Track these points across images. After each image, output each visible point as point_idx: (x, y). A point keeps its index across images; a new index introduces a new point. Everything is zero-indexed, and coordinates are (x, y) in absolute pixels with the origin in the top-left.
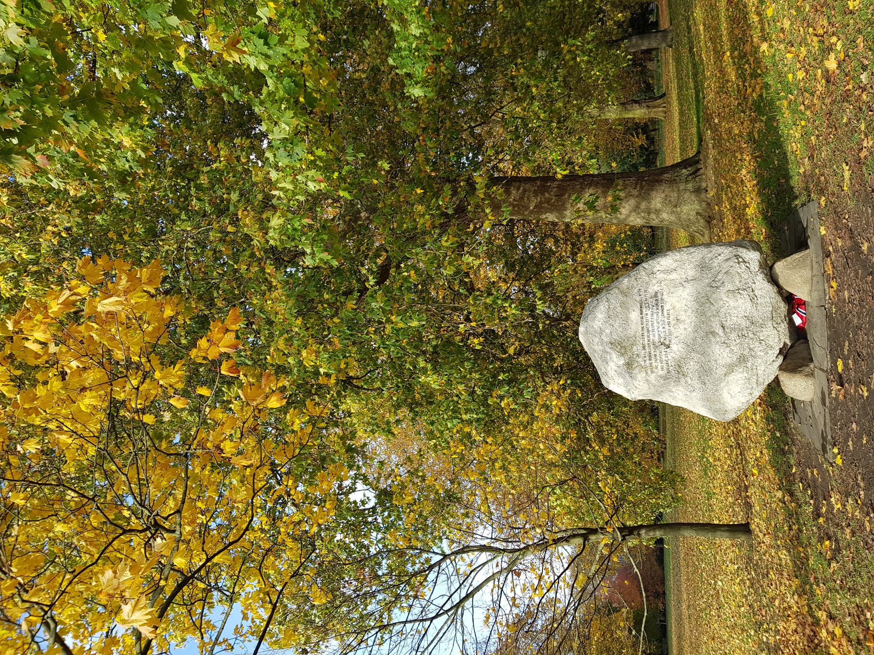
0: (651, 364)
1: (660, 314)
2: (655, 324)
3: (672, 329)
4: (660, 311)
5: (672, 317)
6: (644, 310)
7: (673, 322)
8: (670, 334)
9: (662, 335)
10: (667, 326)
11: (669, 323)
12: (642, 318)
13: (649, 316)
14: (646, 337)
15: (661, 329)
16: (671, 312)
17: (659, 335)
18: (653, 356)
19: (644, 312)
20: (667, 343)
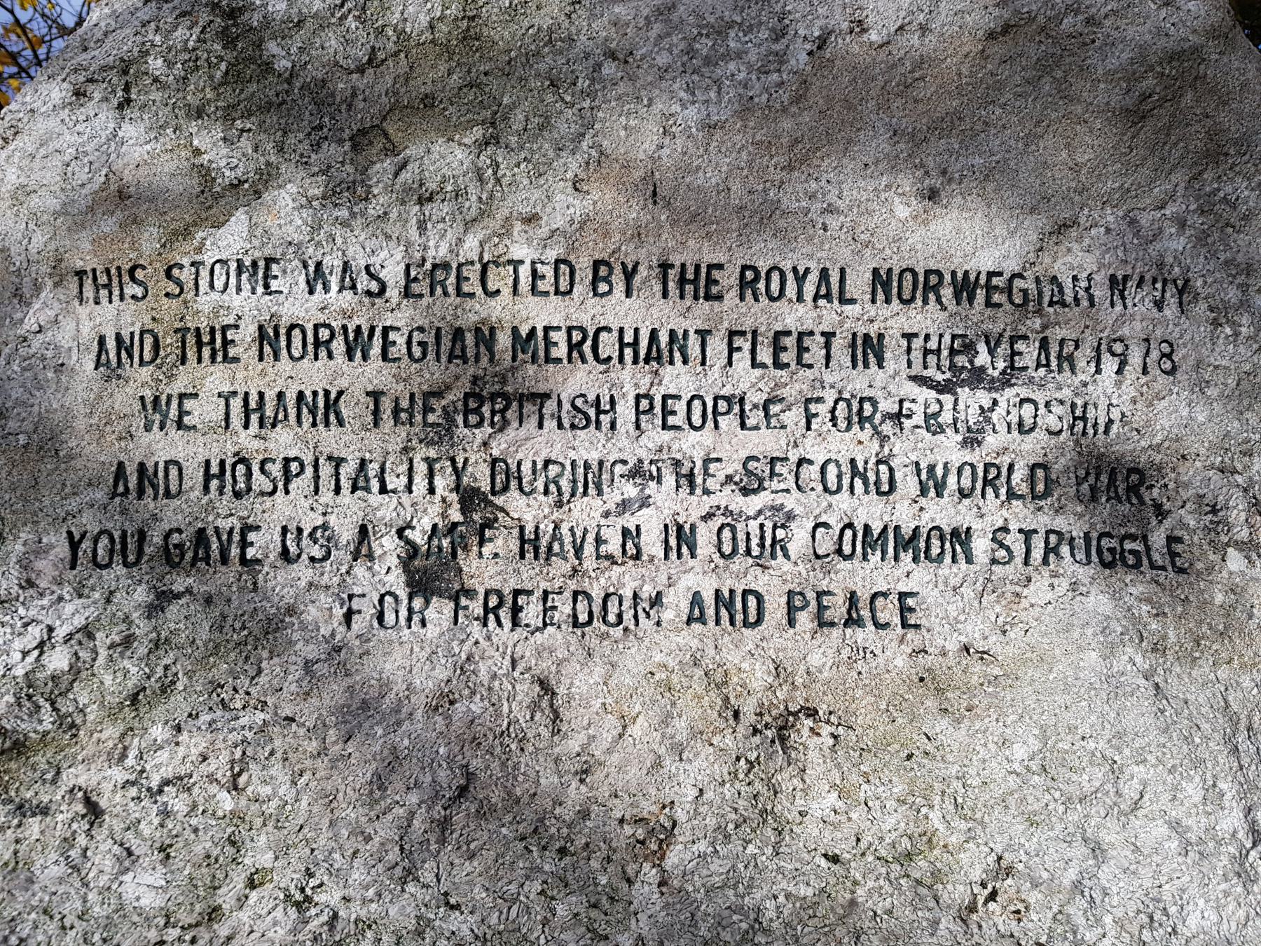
0: (214, 343)
1: (870, 511)
2: (734, 445)
3: (667, 643)
4: (904, 514)
5: (820, 653)
6: (926, 319)
7: (749, 659)
8: (595, 616)
9: (585, 512)
10: (698, 578)
11: (736, 609)
12: (831, 289)
13: (858, 382)
14: (584, 310)
15: (668, 501)
16: (892, 653)
17: (592, 478)
18: (313, 375)
19: (894, 320)
20: (486, 568)
